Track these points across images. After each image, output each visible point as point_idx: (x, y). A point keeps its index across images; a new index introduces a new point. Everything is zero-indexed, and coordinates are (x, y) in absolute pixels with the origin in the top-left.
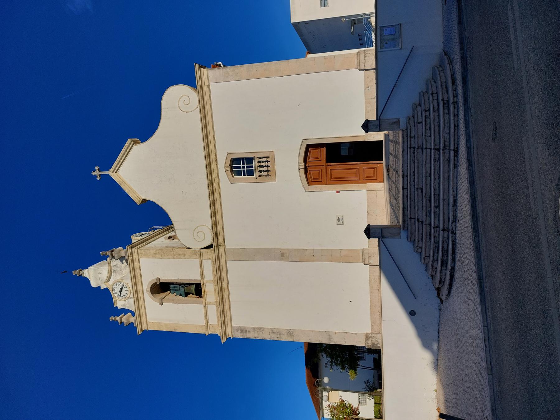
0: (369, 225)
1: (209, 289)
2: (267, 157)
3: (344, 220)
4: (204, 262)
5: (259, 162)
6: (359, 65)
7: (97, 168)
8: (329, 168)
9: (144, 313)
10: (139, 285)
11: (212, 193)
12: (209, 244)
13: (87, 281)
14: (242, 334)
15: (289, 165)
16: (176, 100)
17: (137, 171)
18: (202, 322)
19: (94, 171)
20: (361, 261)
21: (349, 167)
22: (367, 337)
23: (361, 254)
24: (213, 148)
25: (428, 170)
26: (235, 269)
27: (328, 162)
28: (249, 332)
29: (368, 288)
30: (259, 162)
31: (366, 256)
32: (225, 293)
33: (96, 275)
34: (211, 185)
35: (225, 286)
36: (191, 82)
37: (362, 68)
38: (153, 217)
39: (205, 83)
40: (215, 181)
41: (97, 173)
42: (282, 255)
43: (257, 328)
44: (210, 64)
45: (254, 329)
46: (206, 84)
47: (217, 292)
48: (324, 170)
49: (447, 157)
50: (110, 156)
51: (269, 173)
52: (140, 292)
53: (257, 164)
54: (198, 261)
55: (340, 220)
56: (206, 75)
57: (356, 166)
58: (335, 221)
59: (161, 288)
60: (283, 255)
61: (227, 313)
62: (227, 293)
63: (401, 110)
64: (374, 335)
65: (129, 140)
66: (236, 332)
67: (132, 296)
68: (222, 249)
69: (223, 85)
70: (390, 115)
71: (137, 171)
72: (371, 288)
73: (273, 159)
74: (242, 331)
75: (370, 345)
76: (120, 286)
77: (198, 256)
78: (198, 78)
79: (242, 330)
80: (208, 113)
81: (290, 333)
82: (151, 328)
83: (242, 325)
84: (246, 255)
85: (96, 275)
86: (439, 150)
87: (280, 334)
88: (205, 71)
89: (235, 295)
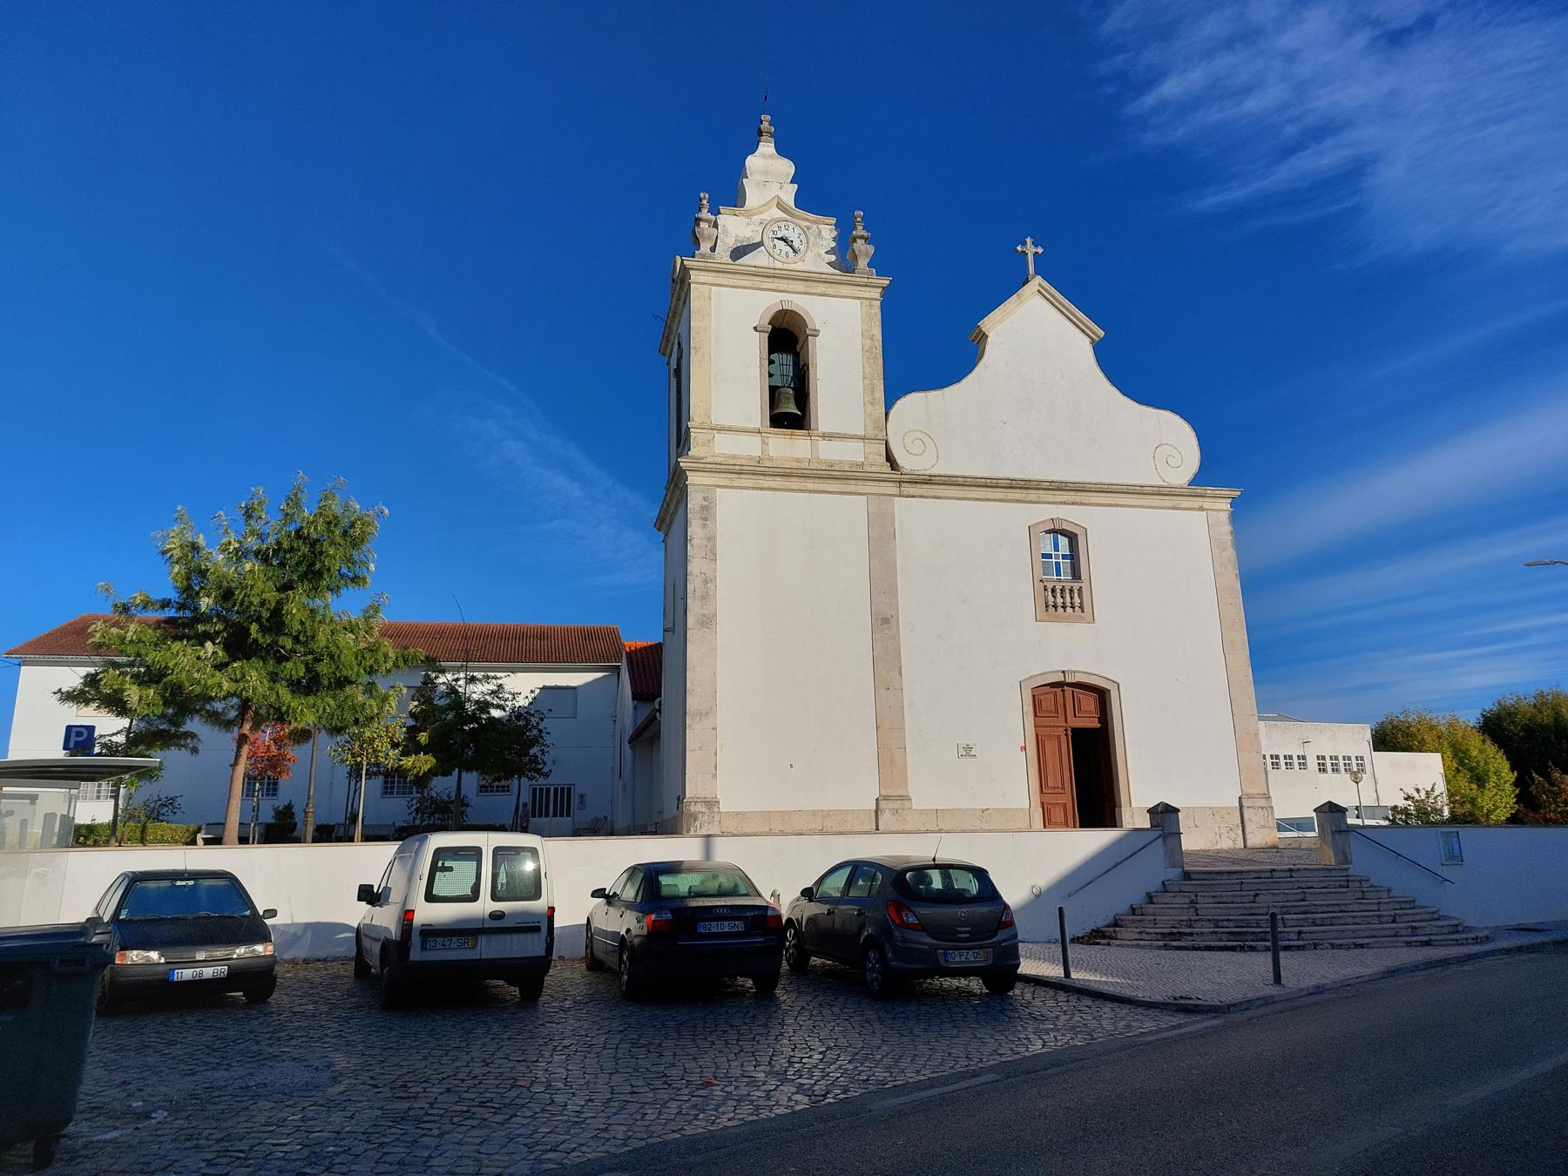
0: (1176, 810)
1: (788, 447)
2: (1081, 607)
3: (969, 759)
4: (859, 445)
5: (1071, 591)
6: (1250, 797)
7: (1040, 250)
8: (1061, 732)
9: (731, 282)
10: (800, 286)
11: (1012, 485)
12: (900, 461)
13: (753, 150)
14: (697, 508)
15: (1072, 651)
16: (1167, 443)
17: (1036, 336)
18: (718, 418)
19: (1035, 244)
20: (884, 793)
21: (1067, 774)
22: (711, 803)
23: (899, 792)
24: (1093, 500)
25: (1350, 908)
26: (847, 512)
27: (1074, 730)
28: (704, 526)
29: (824, 805)
30: (1071, 591)
31: (898, 805)
32: (794, 483)
33: (768, 173)
34: (1027, 485)
35: (810, 485)
36: (1204, 477)
37: (1245, 802)
38: (929, 347)
39: (1207, 504)
40: (1033, 495)
41: (1031, 249)
42: (884, 623)
43: (714, 545)
44: (1238, 514)
45: (711, 538)
46: (1206, 506)
47: (795, 465)
48: (1051, 722)
49: (1403, 932)
50: (1078, 287)
51: (1051, 609)
52: (783, 285)
53: (1068, 586)
54: (861, 433)
55: (968, 751)
56: (1219, 505)
57: (1068, 788)
58: (964, 742)
59: (786, 337)
60: (886, 621)
61: (746, 481)
62: (793, 486)
63: (1363, 862)
64: (717, 817)
65: (1102, 333)
66: (701, 495)
67: (779, 265)
68: (891, 489)
69: (1198, 536)
70: (1357, 849)
71: (1036, 336)
72: (826, 815)
73: (1081, 620)
74: (704, 508)
75: (692, 808)
76: (796, 244)
77: (871, 433)
78: (1210, 491)
79: (707, 511)
80: (1156, 501)
81: (708, 621)
82: (695, 291)
83: (720, 510)
84: (882, 538)
85: (768, 173)
86: (1394, 921)
87: (703, 598)
88: (1225, 505)
89: (791, 504)
